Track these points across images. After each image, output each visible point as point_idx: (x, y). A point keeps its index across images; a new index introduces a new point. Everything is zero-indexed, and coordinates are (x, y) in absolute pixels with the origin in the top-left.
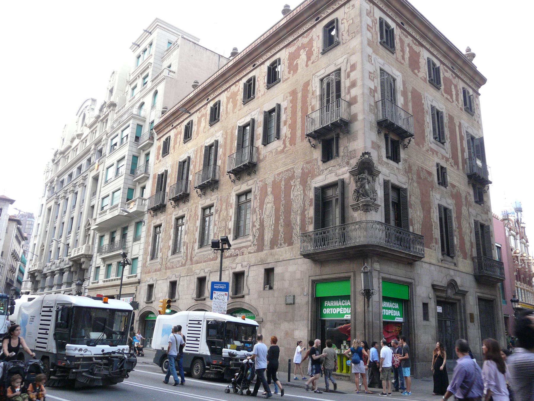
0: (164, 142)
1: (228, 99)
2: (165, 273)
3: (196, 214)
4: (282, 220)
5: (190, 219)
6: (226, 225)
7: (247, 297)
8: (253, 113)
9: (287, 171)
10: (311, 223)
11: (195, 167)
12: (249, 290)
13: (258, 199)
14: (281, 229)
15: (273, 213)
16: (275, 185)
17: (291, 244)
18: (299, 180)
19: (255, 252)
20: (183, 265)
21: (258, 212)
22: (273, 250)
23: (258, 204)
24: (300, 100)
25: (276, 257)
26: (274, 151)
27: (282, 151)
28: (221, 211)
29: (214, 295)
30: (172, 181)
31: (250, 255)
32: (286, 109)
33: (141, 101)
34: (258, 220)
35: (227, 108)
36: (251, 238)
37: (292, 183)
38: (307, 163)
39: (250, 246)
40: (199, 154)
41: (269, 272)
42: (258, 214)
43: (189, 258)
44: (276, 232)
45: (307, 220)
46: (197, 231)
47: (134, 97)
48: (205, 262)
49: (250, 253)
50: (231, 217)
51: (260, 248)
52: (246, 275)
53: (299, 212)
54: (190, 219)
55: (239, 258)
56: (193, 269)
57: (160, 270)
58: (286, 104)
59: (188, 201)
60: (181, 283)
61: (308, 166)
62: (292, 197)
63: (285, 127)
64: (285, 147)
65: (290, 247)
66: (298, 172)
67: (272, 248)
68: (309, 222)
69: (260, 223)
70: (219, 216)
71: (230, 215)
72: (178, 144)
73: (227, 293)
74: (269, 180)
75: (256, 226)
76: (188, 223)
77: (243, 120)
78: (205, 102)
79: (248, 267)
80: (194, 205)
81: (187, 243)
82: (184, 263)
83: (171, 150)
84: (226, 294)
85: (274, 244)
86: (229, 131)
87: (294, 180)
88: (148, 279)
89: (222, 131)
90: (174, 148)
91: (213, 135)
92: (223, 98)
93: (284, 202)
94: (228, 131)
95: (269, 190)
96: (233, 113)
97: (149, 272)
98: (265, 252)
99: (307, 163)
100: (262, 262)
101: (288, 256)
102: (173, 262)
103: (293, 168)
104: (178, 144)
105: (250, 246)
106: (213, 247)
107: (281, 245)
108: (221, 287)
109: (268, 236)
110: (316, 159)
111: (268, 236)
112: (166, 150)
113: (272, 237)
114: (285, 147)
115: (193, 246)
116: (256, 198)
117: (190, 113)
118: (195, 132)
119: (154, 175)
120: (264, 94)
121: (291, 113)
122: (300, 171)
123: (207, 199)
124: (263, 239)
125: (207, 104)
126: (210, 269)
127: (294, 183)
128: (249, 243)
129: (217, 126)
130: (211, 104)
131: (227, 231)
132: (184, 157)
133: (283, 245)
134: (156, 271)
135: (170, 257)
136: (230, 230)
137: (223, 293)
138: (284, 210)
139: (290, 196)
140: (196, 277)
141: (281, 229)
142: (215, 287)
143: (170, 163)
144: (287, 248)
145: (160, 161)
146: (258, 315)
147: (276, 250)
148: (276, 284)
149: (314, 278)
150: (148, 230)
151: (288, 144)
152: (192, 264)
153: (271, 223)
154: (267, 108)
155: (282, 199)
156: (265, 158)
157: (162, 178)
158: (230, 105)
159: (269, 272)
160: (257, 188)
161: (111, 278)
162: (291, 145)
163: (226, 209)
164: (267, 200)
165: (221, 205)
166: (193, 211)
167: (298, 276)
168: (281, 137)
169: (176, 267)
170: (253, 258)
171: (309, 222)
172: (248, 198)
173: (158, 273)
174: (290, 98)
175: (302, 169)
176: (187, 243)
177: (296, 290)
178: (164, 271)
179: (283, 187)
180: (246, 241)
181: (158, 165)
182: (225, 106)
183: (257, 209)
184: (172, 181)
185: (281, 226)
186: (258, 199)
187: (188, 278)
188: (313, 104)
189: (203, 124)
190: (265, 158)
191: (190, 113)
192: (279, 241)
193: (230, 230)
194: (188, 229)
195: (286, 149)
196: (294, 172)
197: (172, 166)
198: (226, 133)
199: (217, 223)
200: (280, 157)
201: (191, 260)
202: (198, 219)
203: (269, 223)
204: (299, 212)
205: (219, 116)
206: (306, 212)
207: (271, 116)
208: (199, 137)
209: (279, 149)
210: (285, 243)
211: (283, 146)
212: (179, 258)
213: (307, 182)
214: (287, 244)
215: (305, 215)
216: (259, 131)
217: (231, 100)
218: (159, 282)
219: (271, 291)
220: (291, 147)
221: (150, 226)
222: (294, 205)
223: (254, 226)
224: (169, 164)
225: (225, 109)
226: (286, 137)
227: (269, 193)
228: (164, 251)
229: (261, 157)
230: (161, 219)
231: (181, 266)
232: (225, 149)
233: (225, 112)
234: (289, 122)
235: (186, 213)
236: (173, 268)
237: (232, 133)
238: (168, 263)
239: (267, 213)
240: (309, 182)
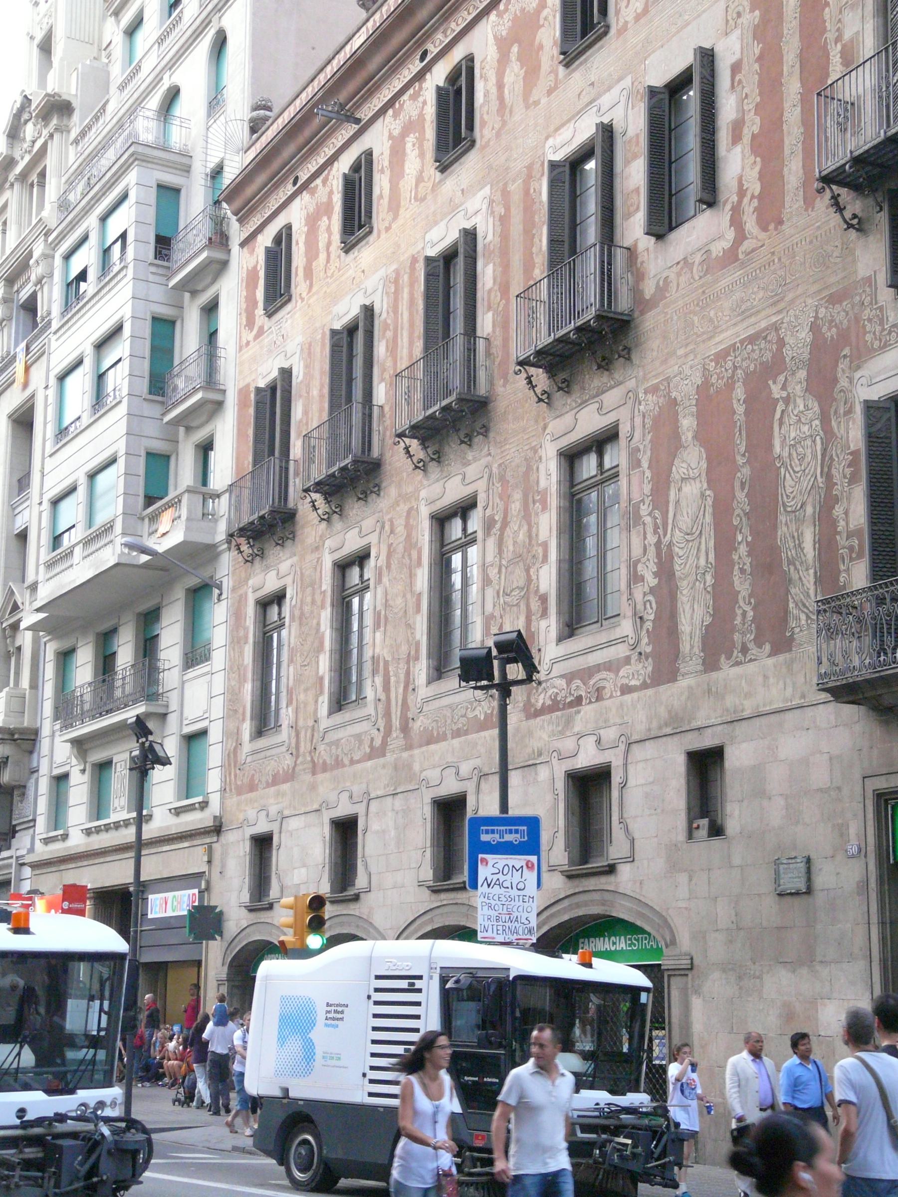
0: (268, 250)
1: (503, 45)
2: (313, 787)
3: (410, 544)
4: (743, 549)
5: (388, 566)
6: (529, 580)
7: (625, 872)
8: (606, 100)
9: (752, 339)
10: (860, 556)
11: (393, 350)
12: (633, 841)
13: (645, 464)
14: (742, 586)
15: (708, 518)
16: (709, 401)
17: (782, 643)
18: (802, 374)
19: (644, 686)
20: (377, 752)
21: (648, 520)
22: (714, 675)
23: (647, 488)
24: (795, 23)
25: (730, 701)
26: (698, 258)
27: (731, 256)
28: (505, 524)
29: (483, 872)
30: (309, 410)
31: (628, 698)
32: (736, 68)
33: (166, 84)
34: (652, 551)
35: (500, 86)
36: (626, 627)
37: (776, 391)
38: (834, 299)
39: (627, 660)
40: (406, 290)
41: (705, 765)
42: (650, 530)
43: (396, 722)
44: (722, 598)
45: (842, 540)
46: (418, 610)
47: (138, 69)
48: (457, 734)
49: (626, 690)
50: (545, 546)
51: (666, 670)
52: (616, 778)
53: (809, 510)
54: (388, 566)
55: (588, 711)
56: (417, 767)
57: (290, 776)
58: (737, 47)
59: (377, 489)
60: (375, 826)
61: (839, 314)
62: (777, 449)
63: (738, 149)
64: (741, 236)
65: (781, 658)
66: (798, 341)
67: (710, 664)
68: (851, 549)
69: (660, 564)
71: (542, 537)
72: (322, 256)
73: (534, 859)
74: (685, 389)
75: (642, 579)
76: (385, 580)
77: (565, 134)
78: (415, 66)
79: (622, 747)
80: (403, 508)
81: (386, 663)
82: (378, 742)
83: (299, 285)
84: (530, 866)
85: (717, 647)
86: (515, 187)
87: (781, 378)
88: (251, 814)
89: (487, 190)
90: (309, 273)
91: (453, 208)
92: (483, 43)
93: (746, 471)
94: (511, 187)
95: (687, 423)
96: (527, 107)
97: (252, 788)
98: (683, 683)
99: (834, 299)
100: (675, 726)
101: (775, 694)
102: (337, 743)
103: (776, 327)
104: (322, 256)
105: (627, 660)
106: (465, 676)
107: (745, 650)
108: (508, 838)
109: (692, 617)
110: (869, 281)
111: (692, 617)
112: (277, 287)
113: (708, 620)
114: (741, 236)
115: (408, 673)
116: (635, 463)
117: (357, 121)
118: (385, 202)
119: (243, 393)
120: (646, 11)
121: (761, 84)
122: (805, 335)
123: (449, 477)
124: (673, 632)
125: (420, 76)
126: (477, 762)
127: (784, 388)
128: (621, 651)
129: (470, 166)
130: (439, 75)
131: (535, 605)
132: (346, 311)
133: (754, 651)
134: (276, 780)
135: (325, 723)
136: (544, 599)
137: (518, 861)
138: (750, 505)
139: (770, 446)
140: (428, 796)
141: (742, 586)
142: (484, 838)
143: (299, 339)
144: (770, 661)
145: (261, 332)
146: (673, 942)
147: (728, 673)
148: (735, 815)
149: (882, 784)
150: (237, 615)
151: (750, 223)
152: (409, 747)
153: (702, 562)
154: (660, 75)
155: (740, 460)
156: (662, 290)
157: (272, 404)
158: (514, 74)
159: (705, 765)
160: (638, 420)
161: (114, 817)
162: (765, 229)
163: (527, 516)
164: (679, 469)
165: (506, 498)
166: (400, 529)
167: (820, 776)
168: (722, 197)
169: (352, 762)
170: (640, 711)
171: (851, 549)
172: (607, 464)
173: (286, 787)
174: (751, 18)
175: (815, 328)
176: (386, 663)
177: (815, 837)
178: (307, 778)
179: (740, 409)
180: (610, 643)
181: (254, 348)
182: (493, 80)
183: (644, 510)
184: (309, 410)
185: (742, 571)
186: (645, 464)
187: (398, 802)
188: (847, 35)
190: (662, 290)
191: (357, 121)
192: (737, 637)
193: (544, 599)
194: (386, 605)
195: (747, 245)
196: (781, 343)
197: (308, 350)
198: (505, 193)
199: (493, 572)
200: (723, 283)
201: (405, 729)
203: (694, 560)
204: (809, 510)
205: (471, 127)
206: (838, 511)
207: (680, 105)
208: (400, 221)
209: (718, 248)
210: (759, 643)
211: (730, 235)
212: (360, 724)
213: (835, 381)
214: (767, 647)
215: (834, 523)
216: (634, 174)
217: (515, 49)
218: (293, 824)
219: (716, 842)
220: (763, 235)
221: (242, 600)
222: (789, 482)
223: (635, 578)
224: (294, 344)
225: (494, 91)
226: (742, 193)
227: (687, 436)
229: (649, 289)
230: (279, 570)
231: (369, 757)
232: (506, 267)
233: (494, 105)
234: (754, 124)
235: (373, 539)
236: (339, 763)
237: (527, 193)
238: (321, 748)
239: (685, 521)
240: (843, 383)
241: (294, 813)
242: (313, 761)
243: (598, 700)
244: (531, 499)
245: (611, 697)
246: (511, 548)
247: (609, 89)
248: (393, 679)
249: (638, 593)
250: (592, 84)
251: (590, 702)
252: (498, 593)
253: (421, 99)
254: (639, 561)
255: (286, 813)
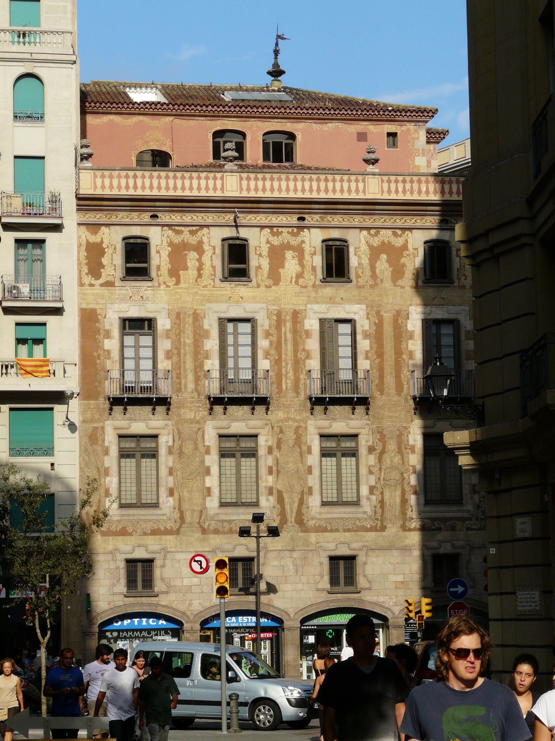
6: (403, 478)
28: (383, 452)
39: (470, 519)
49: (468, 529)
70: (380, 459)
76: (276, 453)
86: (387, 316)
105: (470, 519)
128: (466, 515)
180: (460, 511)
182: (365, 261)
189: (291, 265)
199: (375, 470)
202: (309, 451)
228: (186, 494)
241: (181, 550)
242: (201, 527)
243: (451, 530)
244: (403, 446)
245: (460, 530)
246: (389, 462)
247: (454, 305)
248: (286, 500)
249: (476, 497)
250: (443, 298)
251: (447, 530)
252: (379, 479)
253: (299, 239)
254: (476, 485)
255: (169, 549)
